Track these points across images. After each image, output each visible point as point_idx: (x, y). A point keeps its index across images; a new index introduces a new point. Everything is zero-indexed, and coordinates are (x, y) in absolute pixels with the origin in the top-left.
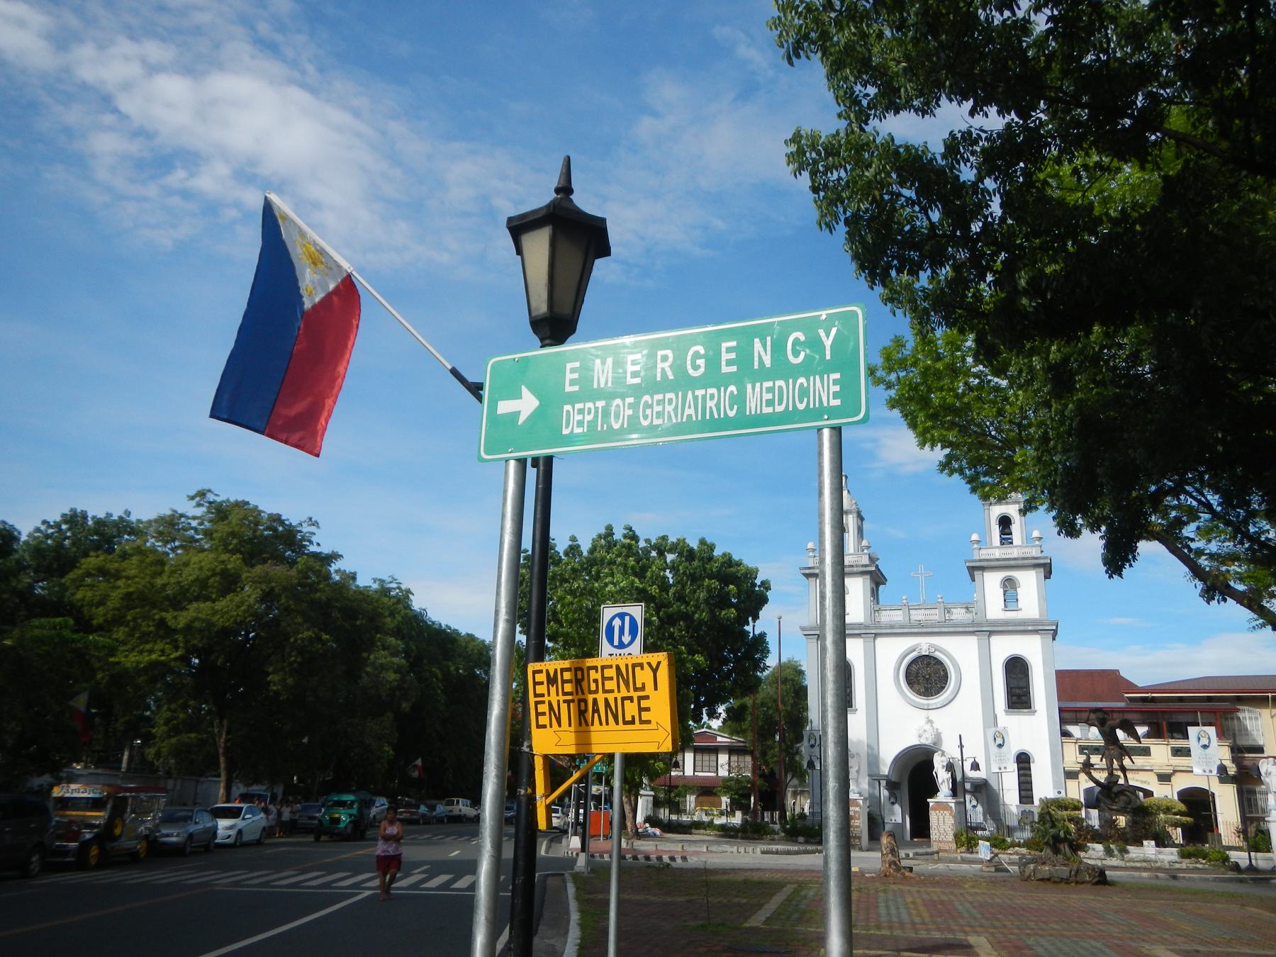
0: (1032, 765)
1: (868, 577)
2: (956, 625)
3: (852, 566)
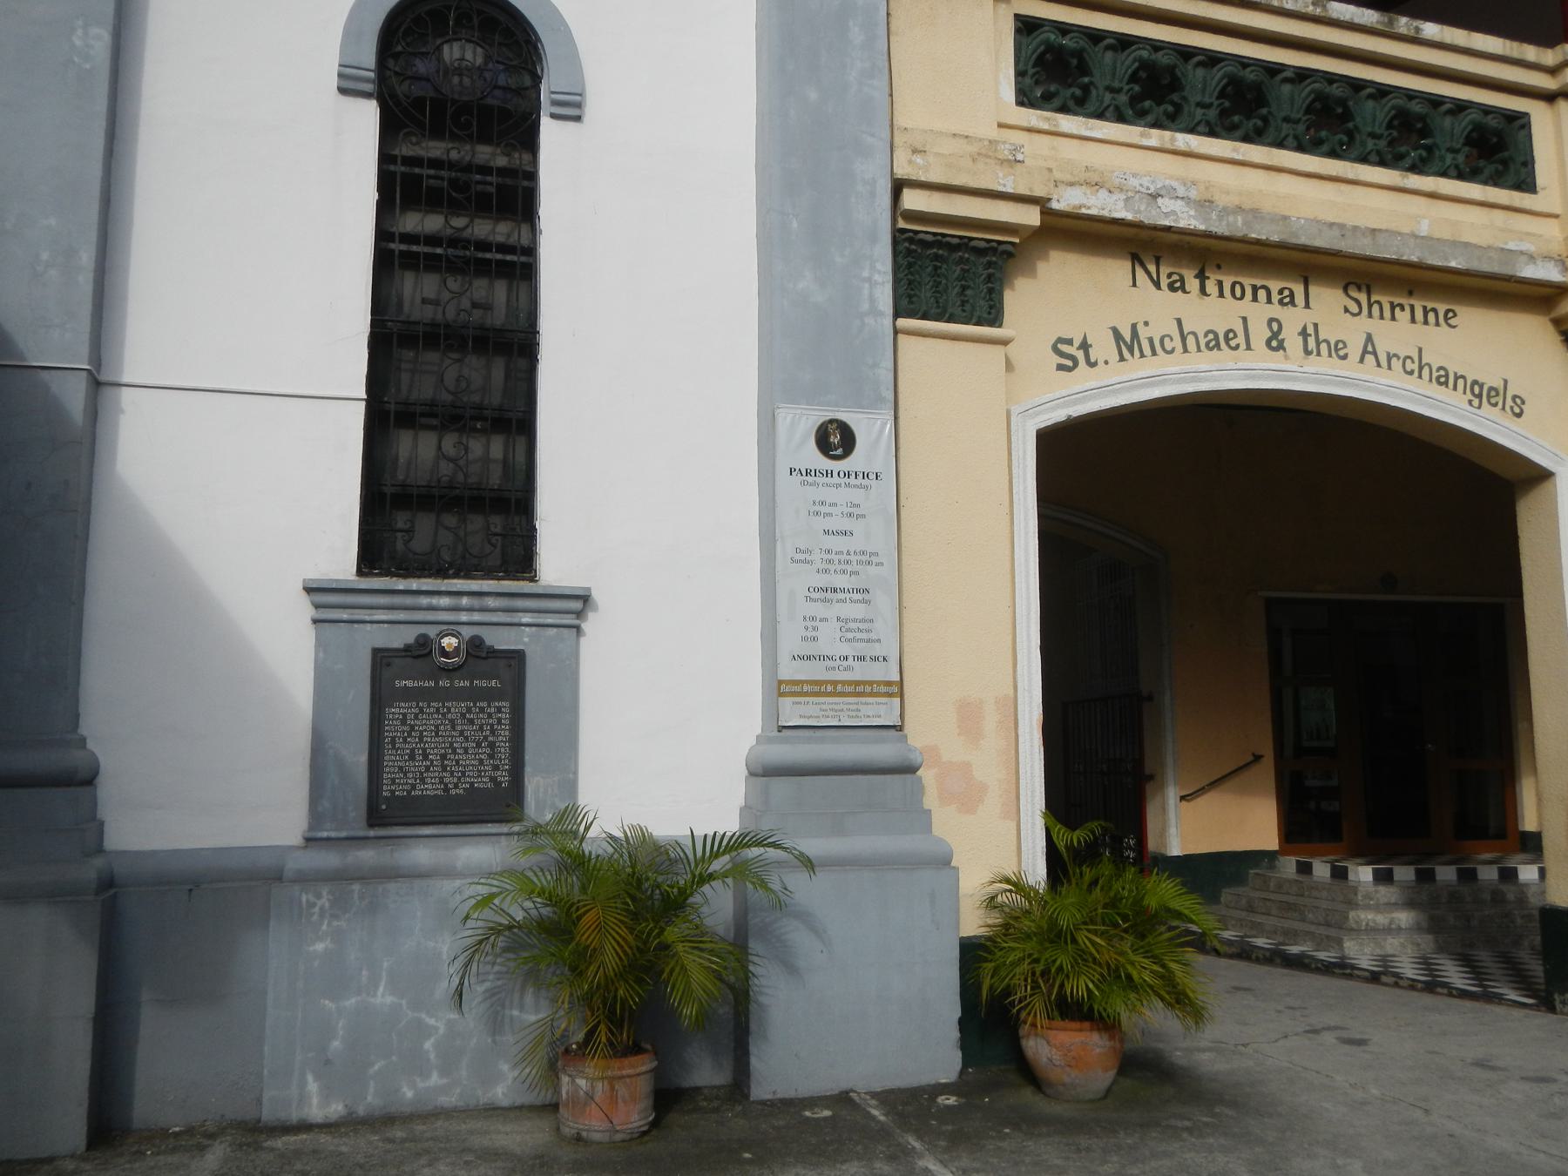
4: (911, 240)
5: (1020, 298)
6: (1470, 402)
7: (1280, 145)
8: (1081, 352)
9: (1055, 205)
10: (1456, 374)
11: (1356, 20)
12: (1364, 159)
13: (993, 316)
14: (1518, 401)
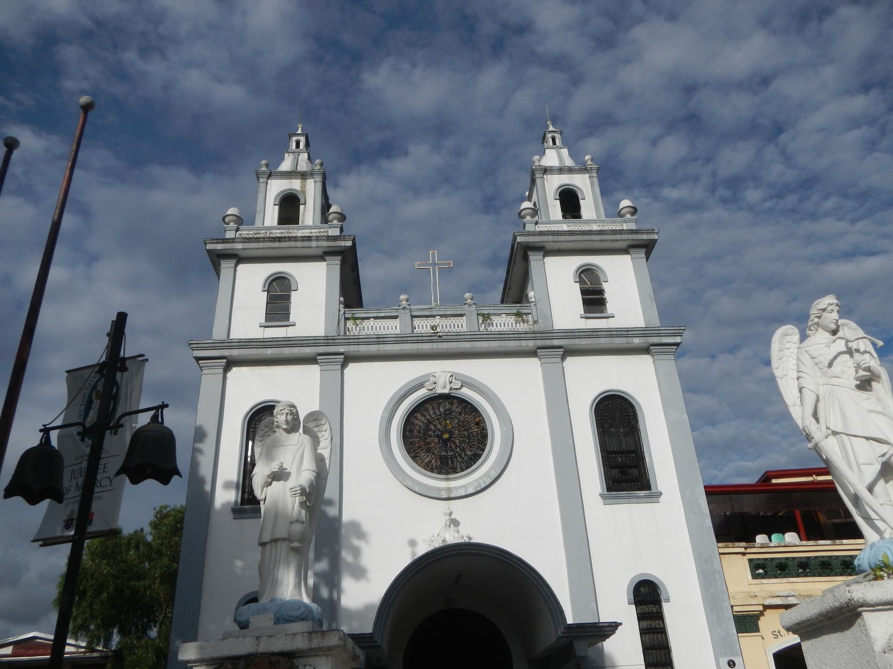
0: (666, 607)
1: (336, 261)
2: (501, 336)
3: (309, 238)
4: (737, 616)
5: (762, 623)
7: (814, 576)
9: (766, 604)
11: (826, 544)
12: (836, 575)
13: (757, 630)
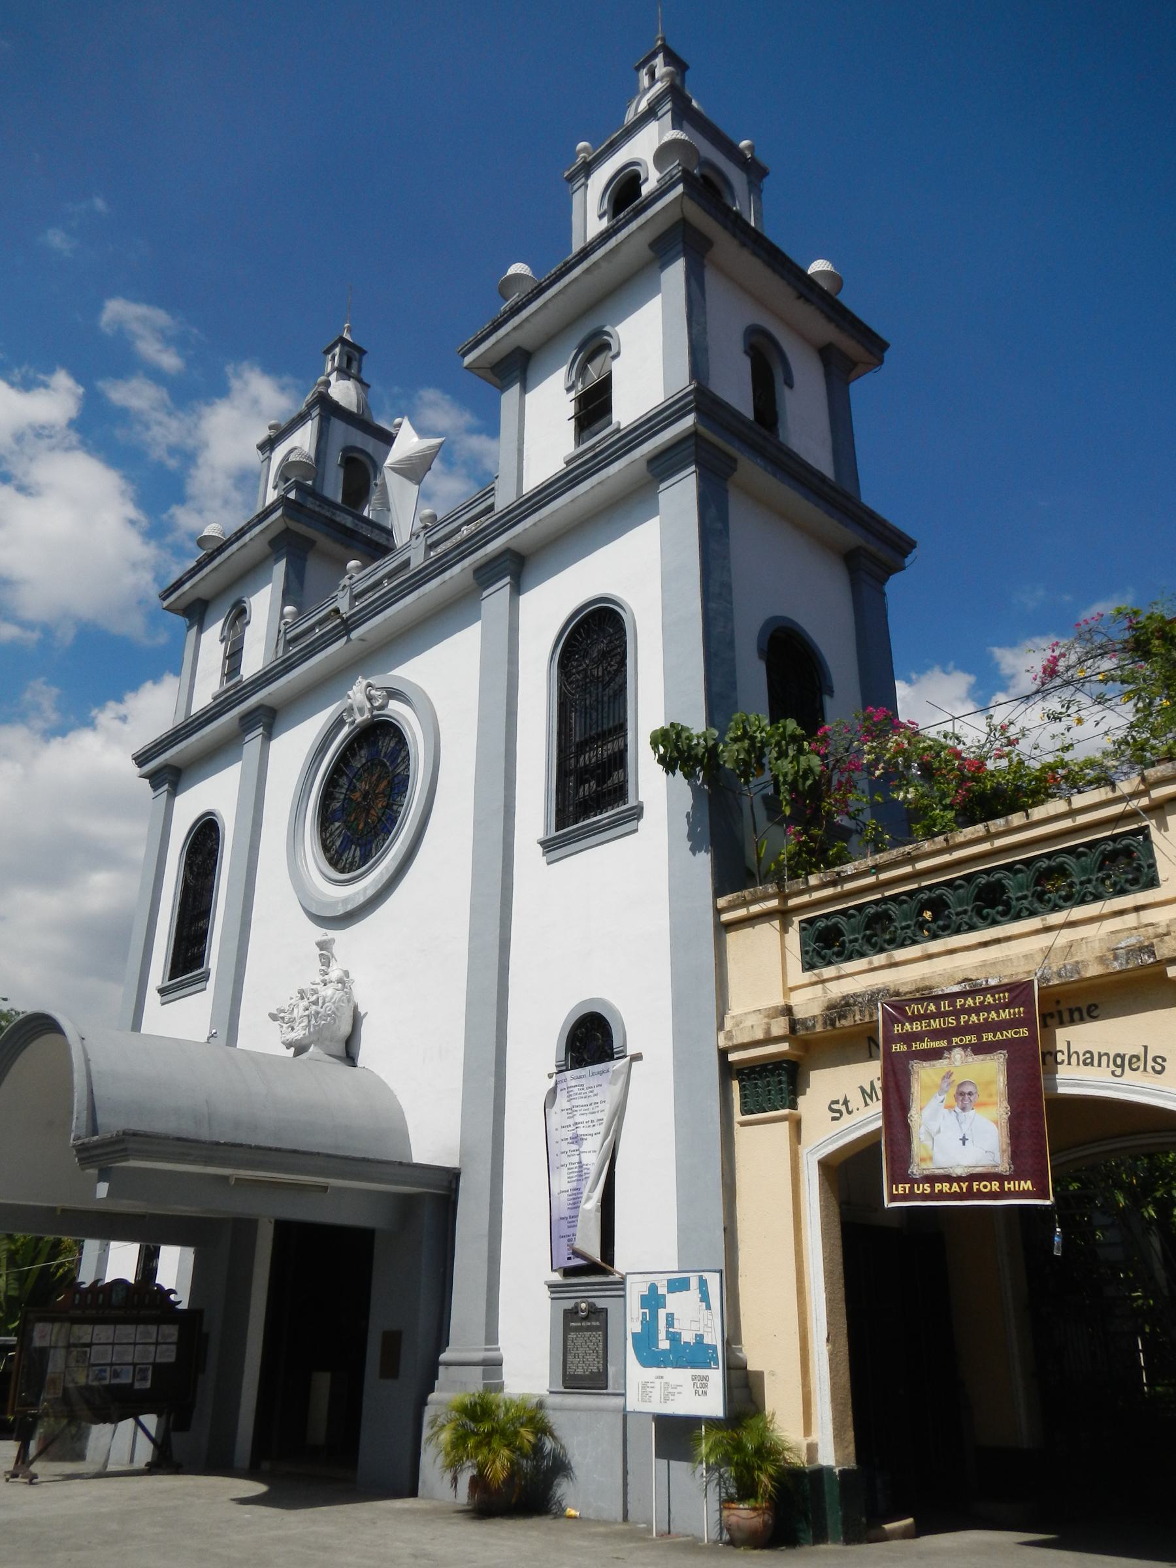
6: (1113, 1073)
8: (844, 1107)
10: (1099, 1053)
14: (1159, 1060)
